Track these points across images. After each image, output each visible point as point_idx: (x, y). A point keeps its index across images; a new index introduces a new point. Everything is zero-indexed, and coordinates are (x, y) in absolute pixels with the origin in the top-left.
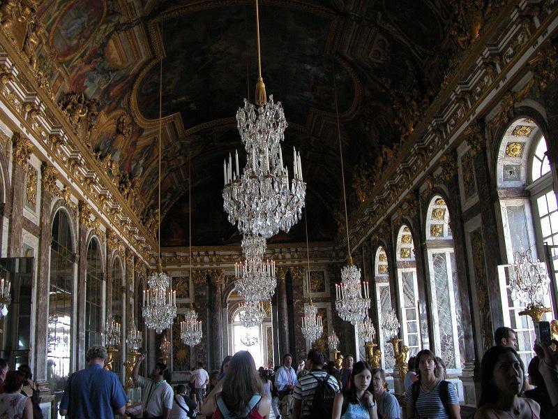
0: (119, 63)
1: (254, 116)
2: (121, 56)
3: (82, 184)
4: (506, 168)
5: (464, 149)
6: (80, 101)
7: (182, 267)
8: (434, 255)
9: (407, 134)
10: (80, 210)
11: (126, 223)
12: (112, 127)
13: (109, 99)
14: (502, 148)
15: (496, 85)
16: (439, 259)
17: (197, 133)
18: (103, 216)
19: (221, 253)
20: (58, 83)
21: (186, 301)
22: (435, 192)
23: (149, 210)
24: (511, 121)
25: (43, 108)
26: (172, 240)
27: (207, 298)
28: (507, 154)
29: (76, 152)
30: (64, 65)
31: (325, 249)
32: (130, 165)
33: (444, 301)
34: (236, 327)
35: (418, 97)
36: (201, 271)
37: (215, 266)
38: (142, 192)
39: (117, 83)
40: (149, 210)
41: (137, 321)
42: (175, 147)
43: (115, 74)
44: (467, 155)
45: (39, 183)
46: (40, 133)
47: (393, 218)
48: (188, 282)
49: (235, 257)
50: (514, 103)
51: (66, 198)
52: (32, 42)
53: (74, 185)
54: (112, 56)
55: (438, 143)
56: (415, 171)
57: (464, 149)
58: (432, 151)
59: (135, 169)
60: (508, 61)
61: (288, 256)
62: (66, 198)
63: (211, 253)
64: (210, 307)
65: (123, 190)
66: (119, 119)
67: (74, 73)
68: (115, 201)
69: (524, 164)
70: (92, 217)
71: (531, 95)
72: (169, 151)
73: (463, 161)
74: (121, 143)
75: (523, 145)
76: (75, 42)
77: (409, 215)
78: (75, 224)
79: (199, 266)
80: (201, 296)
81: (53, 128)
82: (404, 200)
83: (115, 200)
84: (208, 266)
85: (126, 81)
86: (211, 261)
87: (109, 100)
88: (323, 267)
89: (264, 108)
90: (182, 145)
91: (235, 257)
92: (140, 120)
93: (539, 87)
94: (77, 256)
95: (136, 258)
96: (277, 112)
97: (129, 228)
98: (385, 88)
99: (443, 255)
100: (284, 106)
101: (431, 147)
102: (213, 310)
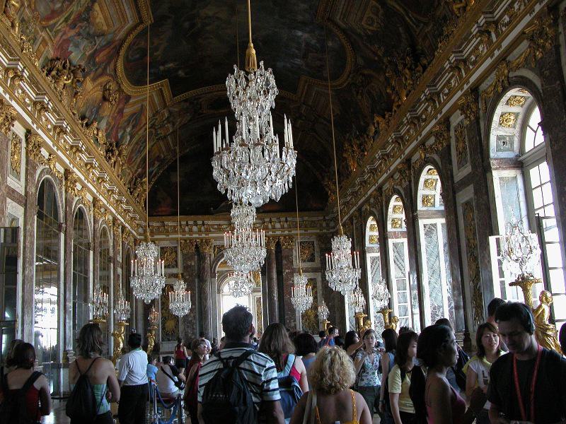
0: (105, 28)
1: (244, 83)
2: (106, 19)
3: (68, 153)
4: (499, 138)
5: (457, 118)
6: (64, 67)
7: (170, 236)
8: (425, 226)
9: (400, 103)
10: (66, 179)
11: (113, 192)
12: (98, 94)
13: (94, 64)
14: (496, 118)
15: (491, 54)
16: (431, 230)
17: (186, 101)
18: (89, 185)
19: (210, 223)
20: (42, 48)
21: (174, 271)
22: (426, 162)
23: (136, 179)
24: (505, 90)
25: (26, 74)
26: (160, 209)
27: (196, 268)
28: (501, 124)
29: (61, 120)
30: (47, 29)
31: (315, 219)
32: (117, 133)
33: (435, 272)
34: (225, 297)
35: (411, 66)
36: (190, 240)
38: (130, 160)
39: (101, 49)
40: (136, 179)
41: (125, 291)
42: (163, 115)
43: (100, 39)
44: (460, 125)
45: (24, 151)
46: (24, 100)
47: (385, 188)
48: (176, 252)
49: (225, 227)
50: (509, 72)
51: (52, 166)
52: (13, 5)
53: (60, 153)
54: (98, 20)
55: (431, 112)
56: (408, 141)
57: (457, 118)
58: (424, 120)
59: (123, 137)
60: (504, 29)
61: (278, 225)
62: (52, 166)
64: (199, 277)
65: (110, 158)
67: (58, 38)
68: (101, 170)
69: (517, 135)
70: (79, 186)
71: (526, 64)
72: (157, 119)
73: (456, 131)
74: (108, 110)
75: (517, 115)
76: (58, 5)
77: (401, 185)
78: (61, 192)
79: (187, 236)
80: (191, 266)
81: (37, 94)
82: (396, 169)
83: (101, 169)
84: (197, 236)
85: (112, 46)
86: (200, 231)
87: (95, 66)
88: (314, 236)
89: (255, 74)
90: (170, 113)
91: (225, 227)
92: (127, 87)
93: (535, 56)
94: (64, 225)
95: (124, 228)
96: (267, 79)
97: (116, 197)
98: (379, 56)
99: (434, 225)
100: (274, 73)
101: (424, 117)
102: (202, 280)
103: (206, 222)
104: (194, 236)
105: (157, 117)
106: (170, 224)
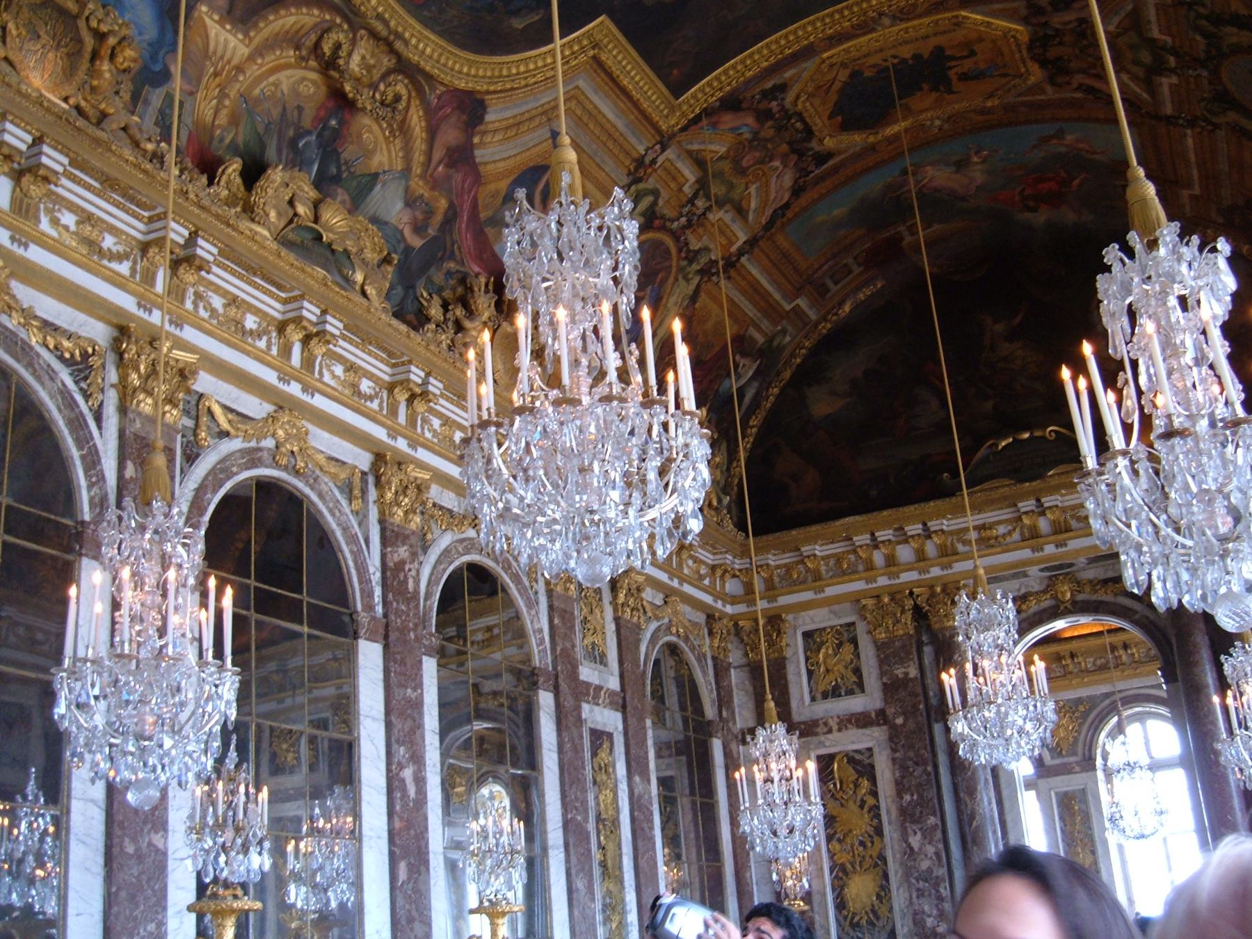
7: (830, 591)
17: (732, 103)
21: (856, 704)
36: (893, 597)
37: (936, 572)
42: (674, 175)
48: (854, 641)
49: (1002, 530)
63: (914, 529)
66: (317, 46)
72: (655, 193)
79: (883, 581)
80: (906, 681)
84: (912, 576)
86: (921, 556)
91: (1002, 530)
103: (933, 525)
104: (906, 577)
105: (650, 183)
106: (819, 550)
